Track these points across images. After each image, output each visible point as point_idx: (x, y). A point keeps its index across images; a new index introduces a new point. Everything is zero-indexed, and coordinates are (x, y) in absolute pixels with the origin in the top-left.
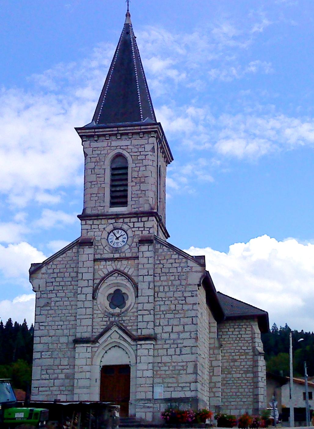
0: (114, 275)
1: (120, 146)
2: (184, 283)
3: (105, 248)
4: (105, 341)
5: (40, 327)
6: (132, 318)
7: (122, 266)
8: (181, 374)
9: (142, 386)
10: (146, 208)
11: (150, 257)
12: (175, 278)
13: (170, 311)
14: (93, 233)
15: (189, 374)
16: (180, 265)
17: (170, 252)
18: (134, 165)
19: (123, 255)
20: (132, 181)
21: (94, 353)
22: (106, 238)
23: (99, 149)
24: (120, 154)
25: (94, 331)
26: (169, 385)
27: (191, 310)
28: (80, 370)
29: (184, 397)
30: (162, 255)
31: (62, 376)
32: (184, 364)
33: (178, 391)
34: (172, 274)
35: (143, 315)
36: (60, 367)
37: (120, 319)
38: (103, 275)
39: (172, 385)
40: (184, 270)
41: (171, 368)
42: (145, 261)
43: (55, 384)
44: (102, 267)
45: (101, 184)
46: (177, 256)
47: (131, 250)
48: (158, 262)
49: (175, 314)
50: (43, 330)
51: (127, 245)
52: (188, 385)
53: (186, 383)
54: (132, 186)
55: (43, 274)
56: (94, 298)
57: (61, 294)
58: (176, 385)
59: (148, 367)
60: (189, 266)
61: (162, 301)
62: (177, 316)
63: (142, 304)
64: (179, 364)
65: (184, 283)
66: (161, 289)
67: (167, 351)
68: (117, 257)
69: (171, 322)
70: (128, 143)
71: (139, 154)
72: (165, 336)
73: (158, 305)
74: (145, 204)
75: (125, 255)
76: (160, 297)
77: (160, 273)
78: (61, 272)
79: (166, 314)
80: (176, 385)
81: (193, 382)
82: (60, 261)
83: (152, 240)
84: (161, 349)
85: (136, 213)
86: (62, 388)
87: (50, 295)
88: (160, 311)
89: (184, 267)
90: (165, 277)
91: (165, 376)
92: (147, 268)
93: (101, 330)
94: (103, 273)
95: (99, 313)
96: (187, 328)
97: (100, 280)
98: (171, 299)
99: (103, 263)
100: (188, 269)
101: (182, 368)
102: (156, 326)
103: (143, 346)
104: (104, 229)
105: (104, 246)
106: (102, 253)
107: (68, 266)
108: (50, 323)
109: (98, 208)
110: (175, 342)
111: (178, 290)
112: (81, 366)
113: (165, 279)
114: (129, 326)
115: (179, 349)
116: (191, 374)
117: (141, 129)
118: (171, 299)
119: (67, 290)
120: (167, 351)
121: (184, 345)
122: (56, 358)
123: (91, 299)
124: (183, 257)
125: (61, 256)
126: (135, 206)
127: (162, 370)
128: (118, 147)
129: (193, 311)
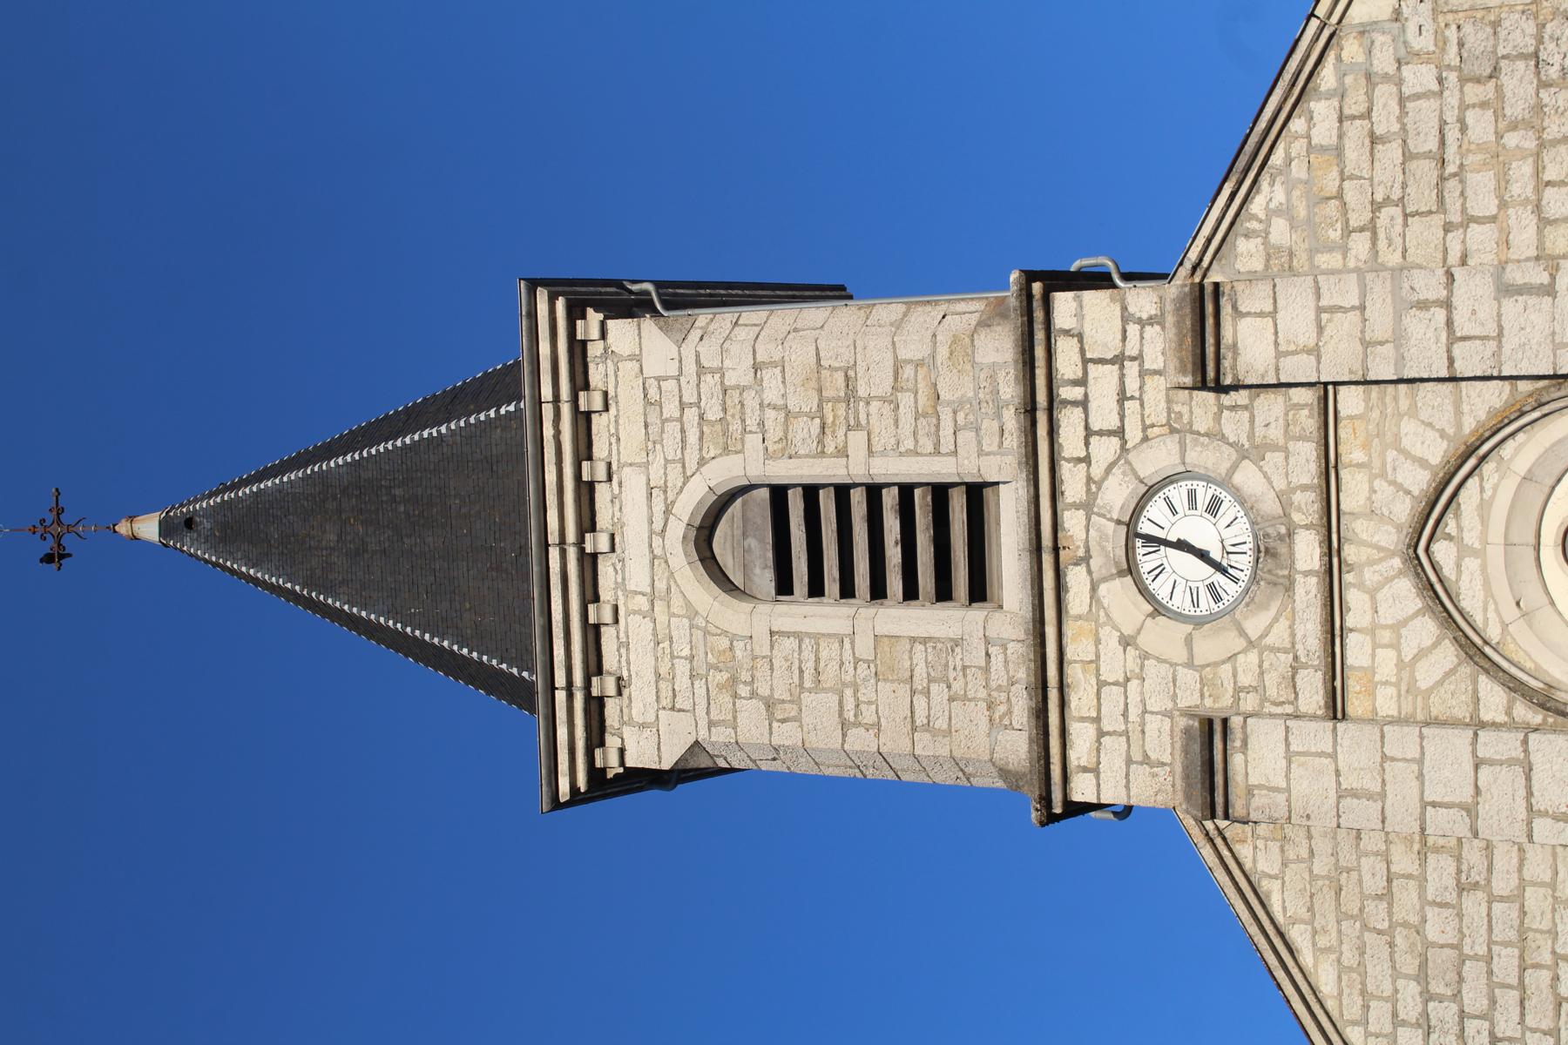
0: (1448, 571)
1: (652, 532)
7: (1378, 504)
11: (1318, 297)
12: (1484, 105)
14: (1153, 723)
16: (1386, 78)
17: (1289, 161)
18: (753, 441)
19: (1306, 507)
20: (843, 452)
22: (1189, 628)
23: (663, 670)
24: (693, 533)
30: (1309, 220)
34: (1452, 135)
38: (1448, 654)
40: (1425, 43)
42: (1342, 329)
44: (1387, 658)
45: (857, 661)
46: (1321, 110)
47: (1275, 448)
51: (1238, 479)
54: (870, 452)
68: (1317, 552)
70: (633, 484)
71: (691, 415)
74: (978, 359)
75: (1304, 488)
77: (1437, 220)
78: (1423, 965)
82: (1342, 969)
85: (1029, 410)
89: (1400, 39)
90: (1472, 178)
92: (1398, 318)
94: (1433, 658)
97: (1483, 678)
99: (1356, 651)
104: (1126, 642)
105: (1241, 643)
107: (1377, 914)
109: (994, 685)
113: (1492, 185)
117: (556, 399)
124: (1331, 57)
125: (1307, 959)
126: (989, 426)
128: (658, 551)
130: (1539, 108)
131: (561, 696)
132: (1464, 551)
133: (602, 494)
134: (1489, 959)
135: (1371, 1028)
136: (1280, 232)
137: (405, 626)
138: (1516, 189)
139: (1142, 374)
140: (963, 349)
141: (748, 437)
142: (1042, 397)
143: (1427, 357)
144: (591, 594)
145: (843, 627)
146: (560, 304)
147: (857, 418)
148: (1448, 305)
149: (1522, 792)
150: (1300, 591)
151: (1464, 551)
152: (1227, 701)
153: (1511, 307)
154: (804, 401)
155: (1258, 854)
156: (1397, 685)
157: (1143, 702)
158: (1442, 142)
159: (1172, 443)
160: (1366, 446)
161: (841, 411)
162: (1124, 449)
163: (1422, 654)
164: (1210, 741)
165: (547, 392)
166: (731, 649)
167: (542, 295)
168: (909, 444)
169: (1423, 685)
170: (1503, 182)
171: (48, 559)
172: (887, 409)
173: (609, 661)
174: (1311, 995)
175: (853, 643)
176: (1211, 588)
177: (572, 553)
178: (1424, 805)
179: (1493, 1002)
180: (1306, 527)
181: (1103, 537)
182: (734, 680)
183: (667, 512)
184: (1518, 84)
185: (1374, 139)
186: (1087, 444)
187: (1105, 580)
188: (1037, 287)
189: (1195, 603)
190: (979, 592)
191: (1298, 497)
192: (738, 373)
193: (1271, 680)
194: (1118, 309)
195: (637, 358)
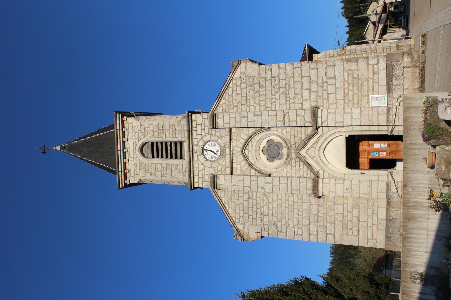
0: (247, 154)
2: (257, 80)
4: (317, 163)
6: (293, 134)
7: (238, 145)
8: (358, 76)
9: (371, 119)
12: (252, 90)
14: (206, 176)
15: (358, 68)
16: (239, 85)
18: (149, 135)
19: (228, 145)
20: (162, 137)
21: (331, 177)
25: (305, 176)
26: (371, 88)
27: (286, 70)
28: (349, 191)
31: (355, 212)
33: (378, 78)
34: (248, 94)
35: (289, 121)
37: (293, 147)
38: (247, 166)
39: (371, 85)
40: (244, 81)
41: (351, 88)
42: (233, 120)
44: (239, 166)
46: (230, 90)
47: (223, 137)
48: (235, 108)
49: (289, 87)
51: (218, 141)
52: (371, 67)
55: (244, 227)
56: (270, 175)
57: (265, 210)
58: (371, 81)
59: (349, 113)
60: (240, 76)
61: (275, 102)
62: (292, 85)
63: (277, 122)
64: (346, 79)
65: (257, 80)
67: (330, 94)
70: (131, 142)
71: (140, 132)
72: (313, 96)
73: (280, 107)
77: (246, 105)
78: (243, 209)
79: (289, 97)
80: (371, 81)
81: (368, 61)
82: (232, 210)
84: (328, 100)
85: (189, 131)
86: (370, 213)
87: (266, 221)
88: (286, 104)
89: (241, 80)
91: (360, 94)
92: (240, 119)
93: (305, 168)
94: (245, 166)
95: (286, 171)
99: (234, 165)
100: (243, 77)
101: (351, 75)
102: (302, 108)
103: (325, 119)
104: (202, 164)
105: (218, 164)
107: (237, 202)
108: (296, 223)
110: (321, 85)
112: (345, 189)
114: (301, 137)
115: (328, 81)
116: (358, 64)
120: (330, 94)
121: (324, 75)
122: (334, 218)
123: (270, 178)
124: (231, 82)
125: (227, 208)
127: (353, 98)
129: (287, 68)
130: (259, 90)
131: (120, 173)
132: (249, 151)
133: (126, 143)
134: (252, 208)
136: (224, 106)
138: (256, 101)
139: (205, 126)
140: (179, 122)
142: (190, 129)
144: (125, 158)
145: (162, 162)
146: (120, 115)
148: (247, 117)
150: (227, 157)
151: (249, 151)
152: (217, 172)
153: (256, 118)
154: (156, 130)
155: (221, 194)
159: (209, 136)
160: (236, 137)
163: (243, 166)
164: (214, 178)
165: (118, 128)
167: (118, 114)
168: (171, 136)
169: (244, 170)
170: (255, 100)
171: (43, 153)
172: (168, 131)
173: (127, 167)
174: (228, 213)
177: (122, 152)
178: (244, 187)
181: (199, 149)
182: (146, 170)
183: (136, 146)
184: (257, 87)
185: (237, 94)
188: (190, 114)
190: (181, 157)
191: (226, 144)
192: (147, 126)
193: (223, 170)
195: (132, 123)
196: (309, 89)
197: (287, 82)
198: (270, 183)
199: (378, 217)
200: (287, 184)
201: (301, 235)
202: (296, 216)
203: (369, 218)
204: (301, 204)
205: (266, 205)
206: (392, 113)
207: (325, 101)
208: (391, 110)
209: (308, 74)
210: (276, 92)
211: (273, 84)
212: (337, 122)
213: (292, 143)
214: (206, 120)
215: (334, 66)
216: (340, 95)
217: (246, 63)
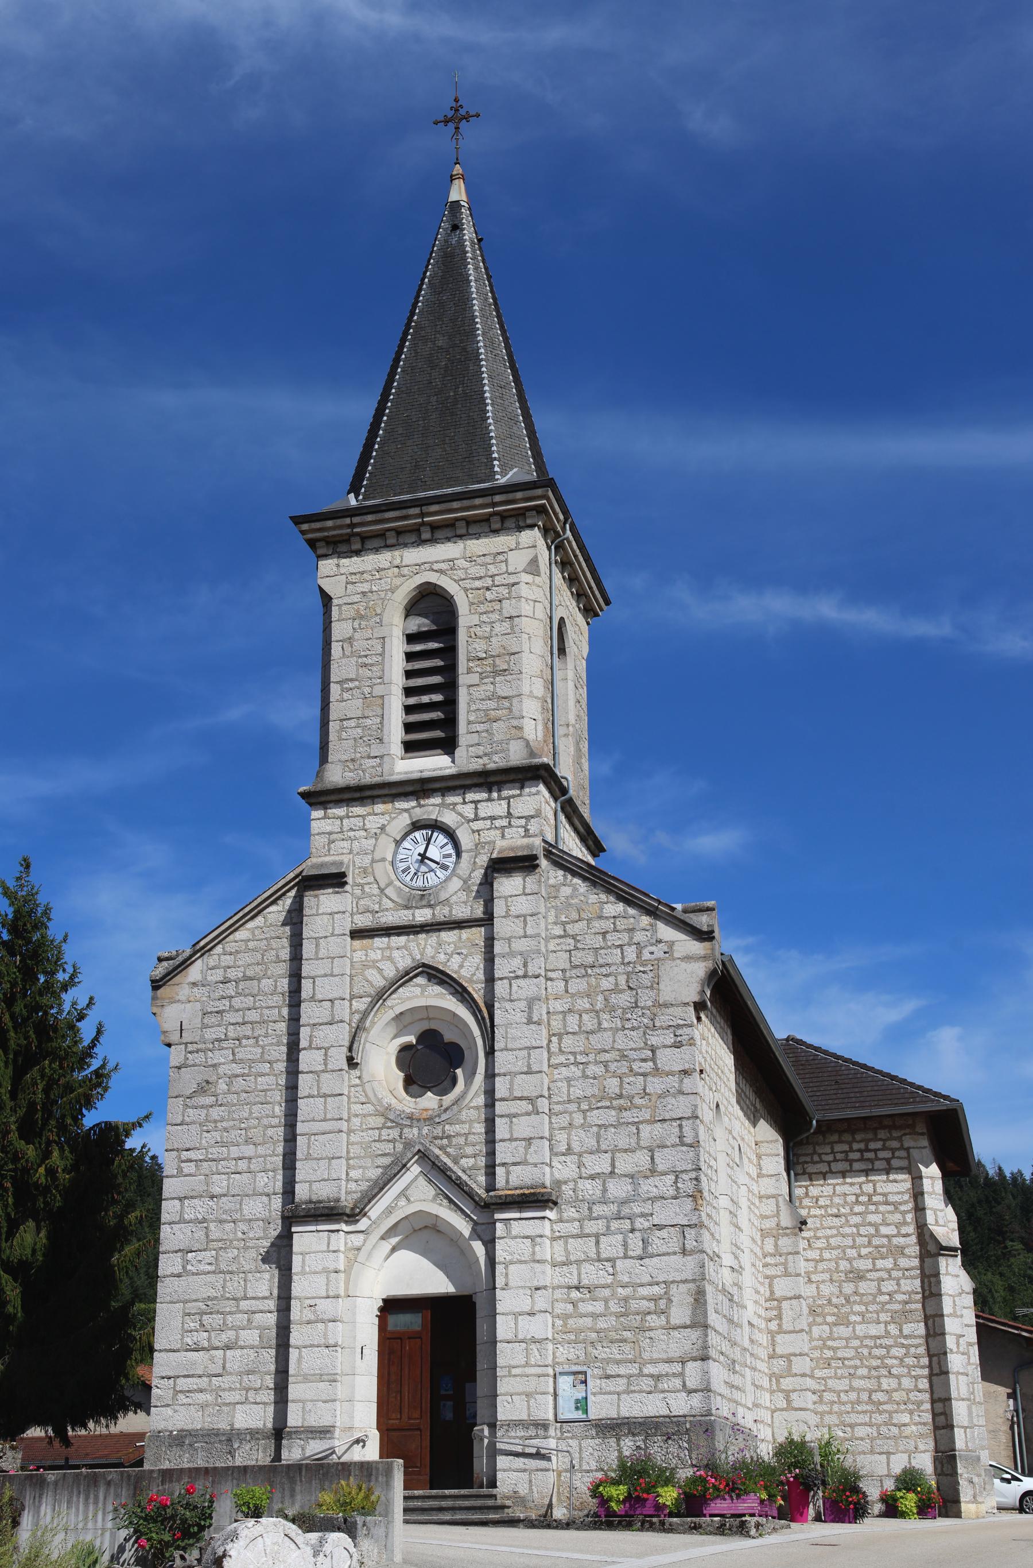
1: (432, 563)
3: (387, 891)
4: (389, 1211)
5: (183, 1165)
8: (651, 1329)
9: (514, 1371)
10: (516, 756)
12: (617, 984)
13: (602, 1099)
15: (675, 1328)
16: (631, 938)
19: (441, 913)
20: (469, 671)
26: (612, 1369)
28: (308, 1315)
29: (666, 1412)
32: (656, 1290)
34: (604, 970)
35: (511, 1116)
36: (244, 1305)
37: (438, 1131)
38: (380, 982)
39: (622, 1370)
41: (614, 1307)
43: (227, 1365)
48: (558, 931)
49: (621, 1109)
50: (190, 1175)
51: (455, 879)
52: (677, 1368)
53: (669, 1361)
58: (634, 1369)
60: (660, 941)
61: (576, 1064)
64: (644, 1291)
65: (646, 999)
66: (572, 1022)
67: (597, 1243)
69: (611, 1138)
72: (590, 1189)
75: (450, 911)
76: (569, 1050)
77: (567, 966)
78: (251, 979)
79: (591, 1109)
80: (634, 1369)
81: (694, 1359)
83: (535, 857)
88: (569, 1101)
93: (374, 1173)
94: (378, 976)
96: (664, 1160)
98: (607, 1056)
99: (380, 942)
100: (659, 951)
104: (383, 828)
106: (376, 907)
108: (215, 1152)
109: (363, 762)
110: (626, 1211)
111: (628, 1025)
112: (312, 1302)
114: (467, 1157)
116: (686, 1327)
117: (494, 505)
118: (607, 1056)
119: (266, 1036)
120: (597, 1243)
125: (250, 925)
126: (480, 751)
129: (681, 1098)
130: (613, 1009)
135: (222, 957)
136: (566, 891)
137: (392, 401)
139: (503, 828)
141: (477, 616)
143: (501, 968)
147: (486, 677)
148: (525, 976)
149: (321, 1021)
150: (406, 912)
153: (523, 1005)
156: (366, 960)
157: (356, 839)
158: (601, 966)
161: (488, 669)
162: (469, 821)
163: (380, 971)
166: (376, 615)
175: (380, 684)
176: (409, 868)
179: (237, 1011)
180: (433, 914)
181: (429, 813)
182: (362, 617)
183: (441, 571)
185: (604, 934)
186: (471, 802)
187: (410, 816)
189: (401, 861)
190: (410, 747)
194: (532, 813)
196: (612, 1173)
197: (638, 1101)
198: (326, 1064)
199: (238, 1406)
200: (325, 1120)
201: (180, 1173)
202: (235, 1151)
203: (234, 1378)
204: (269, 1166)
205: (262, 1053)
206: (531, 1438)
207: (573, 1228)
208: (541, 1432)
209: (660, 1168)
210: (606, 1064)
211: (633, 1055)
212: (506, 1268)
213: (447, 1127)
214: (521, 831)
215: (684, 1252)
216: (592, 1274)
217: (705, 958)
